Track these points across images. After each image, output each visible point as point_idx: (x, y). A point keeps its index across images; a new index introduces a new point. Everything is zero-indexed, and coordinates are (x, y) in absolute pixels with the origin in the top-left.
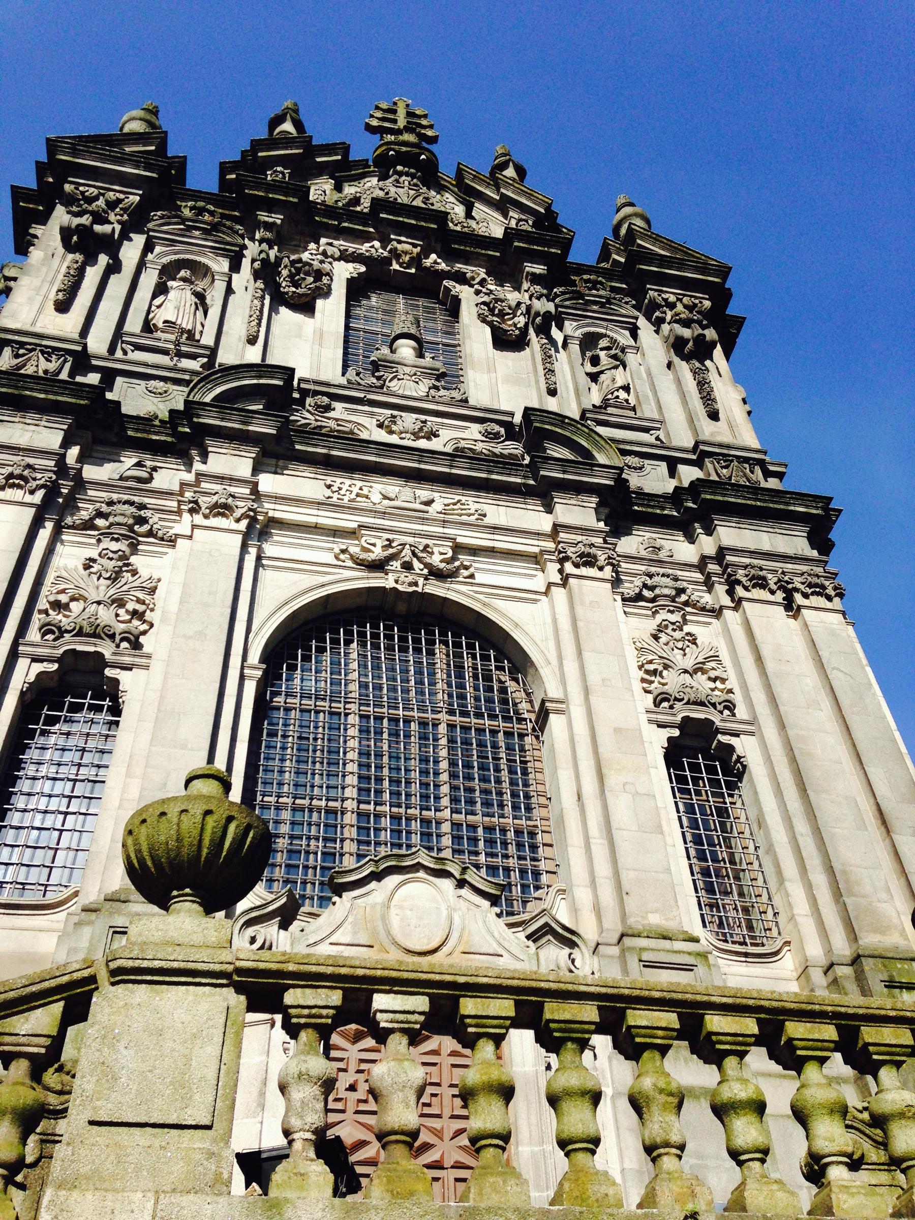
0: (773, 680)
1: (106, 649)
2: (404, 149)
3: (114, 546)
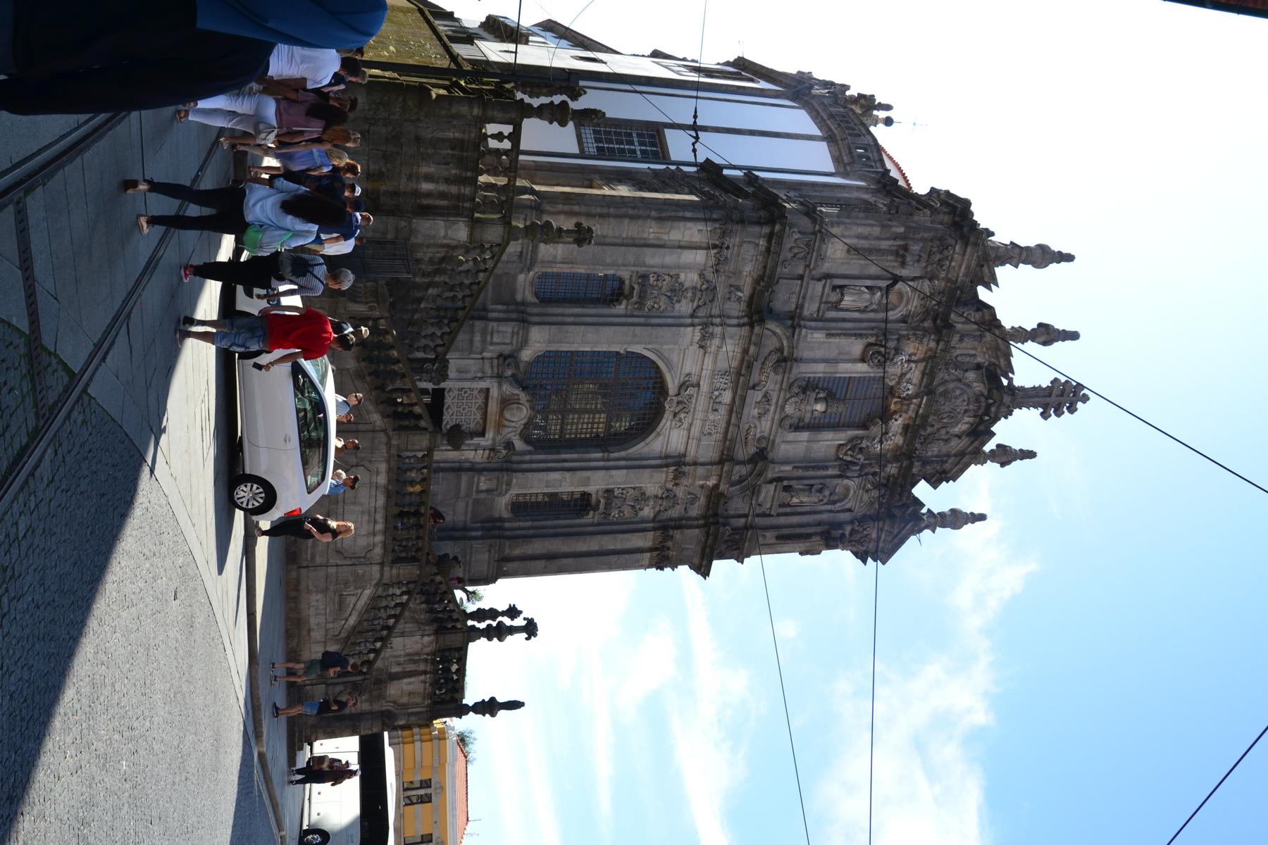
0: (613, 536)
1: (635, 298)
2: (993, 409)
3: (690, 295)
